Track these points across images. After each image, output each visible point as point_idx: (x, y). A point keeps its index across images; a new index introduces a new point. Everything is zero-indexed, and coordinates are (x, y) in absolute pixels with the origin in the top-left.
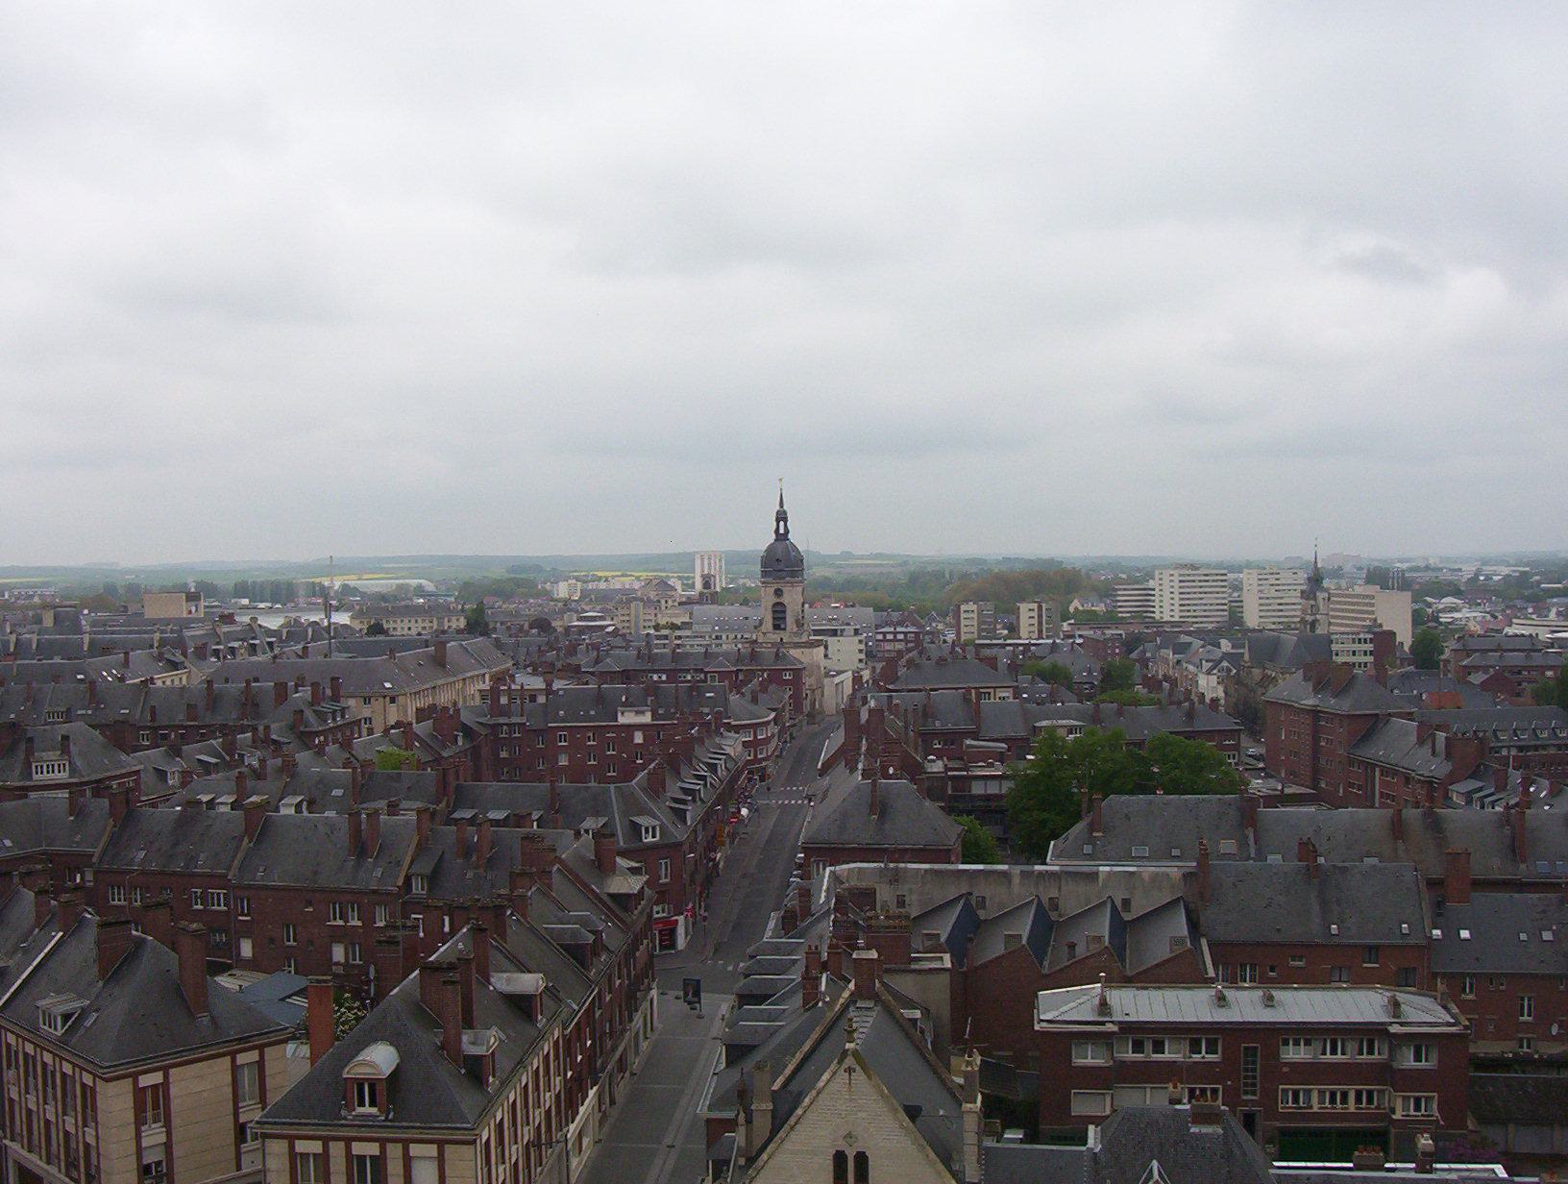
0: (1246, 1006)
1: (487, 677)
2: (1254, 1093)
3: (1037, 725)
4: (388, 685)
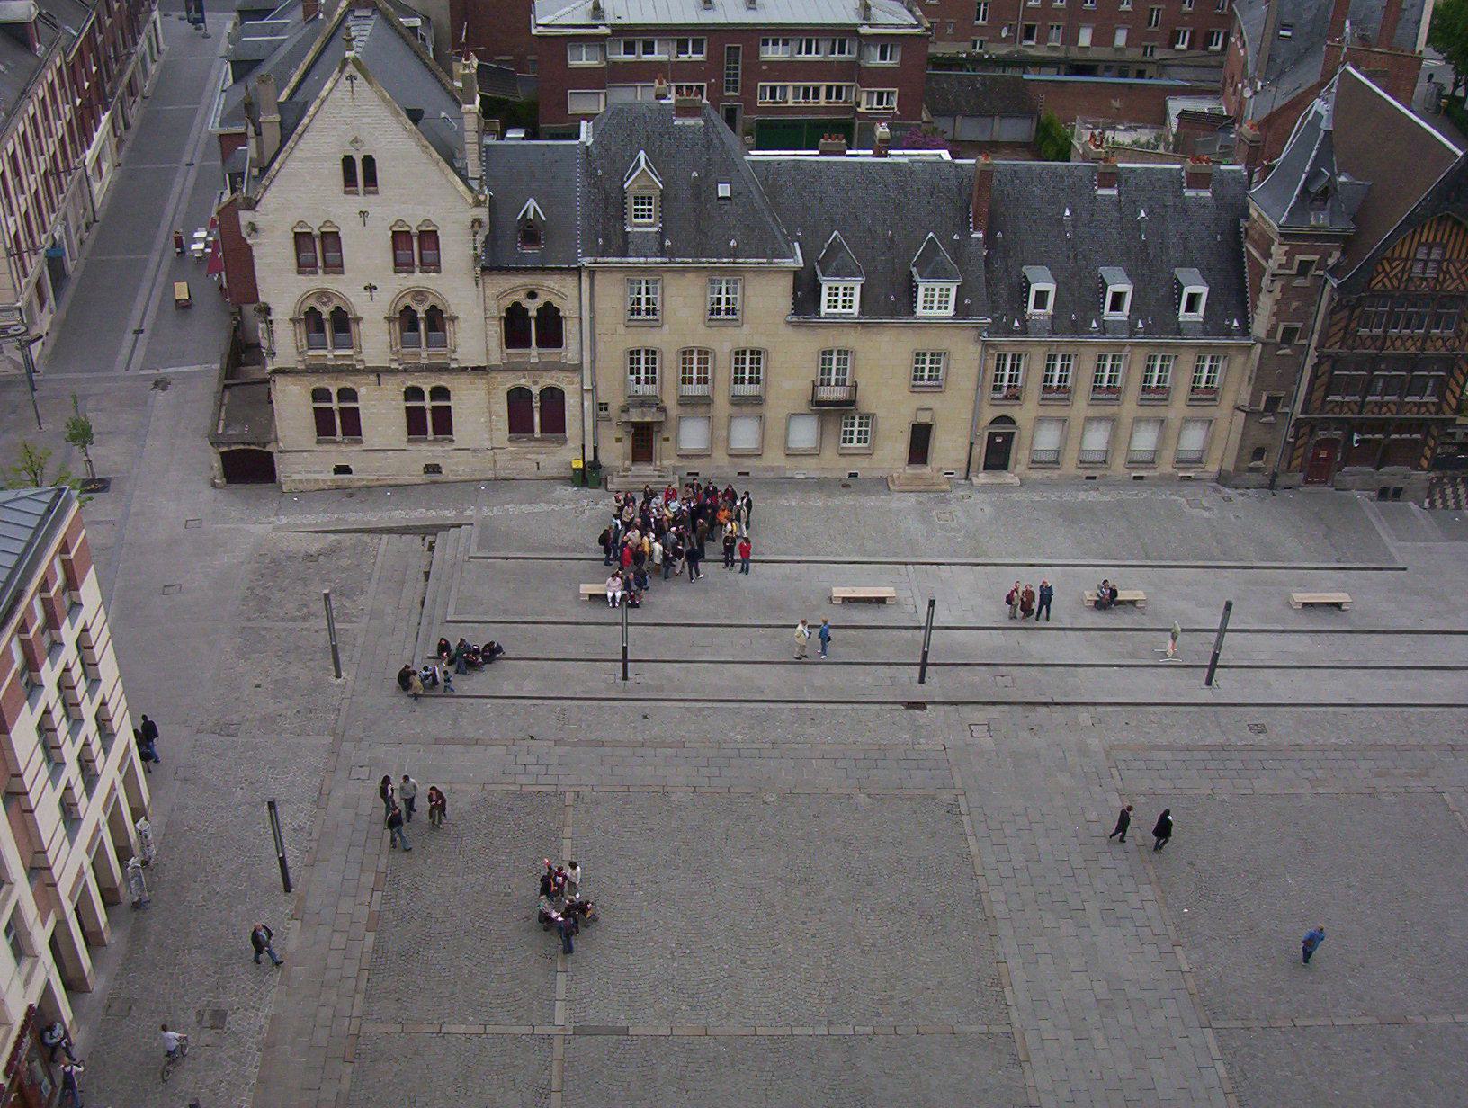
2: (735, 89)
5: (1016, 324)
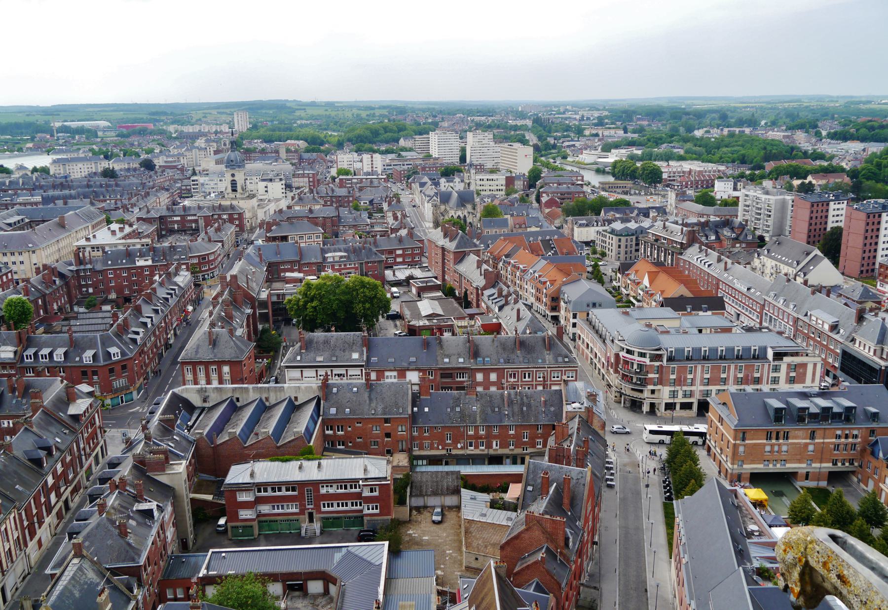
1: (90, 227)
3: (326, 255)
4: (30, 245)
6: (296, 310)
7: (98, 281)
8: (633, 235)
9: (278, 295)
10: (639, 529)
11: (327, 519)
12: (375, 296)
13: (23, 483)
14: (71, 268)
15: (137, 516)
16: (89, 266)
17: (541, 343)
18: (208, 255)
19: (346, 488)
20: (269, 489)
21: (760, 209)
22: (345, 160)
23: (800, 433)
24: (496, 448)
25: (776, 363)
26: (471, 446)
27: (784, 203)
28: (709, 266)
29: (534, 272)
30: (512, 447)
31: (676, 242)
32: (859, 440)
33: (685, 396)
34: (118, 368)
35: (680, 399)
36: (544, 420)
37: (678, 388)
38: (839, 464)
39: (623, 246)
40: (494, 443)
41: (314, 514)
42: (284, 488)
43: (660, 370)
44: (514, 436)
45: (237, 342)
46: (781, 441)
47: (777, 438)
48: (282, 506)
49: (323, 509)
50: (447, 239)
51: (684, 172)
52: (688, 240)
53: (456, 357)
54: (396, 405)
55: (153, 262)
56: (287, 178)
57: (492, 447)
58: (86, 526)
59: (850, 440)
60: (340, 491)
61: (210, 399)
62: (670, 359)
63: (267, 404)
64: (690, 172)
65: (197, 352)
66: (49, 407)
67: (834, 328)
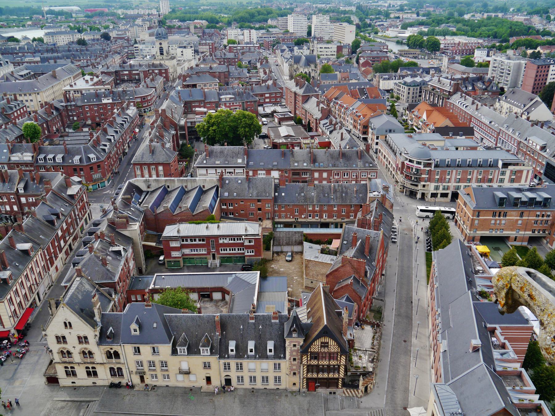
0: (213, 230)
3: (221, 97)
4: (36, 89)
5: (226, 356)
6: (203, 132)
7: (80, 113)
8: (418, 86)
9: (191, 123)
10: (410, 268)
11: (224, 257)
12: (252, 124)
13: (44, 235)
14: (62, 104)
15: (112, 254)
16: (73, 103)
17: (355, 155)
18: (147, 96)
19: (234, 240)
20: (189, 240)
21: (503, 69)
22: (233, 34)
23: (514, 213)
24: (325, 218)
25: (504, 170)
26: (310, 216)
27: (519, 65)
28: (466, 107)
29: (353, 109)
30: (335, 218)
31: (446, 91)
32: (551, 218)
33: (444, 189)
34: (95, 167)
35: (441, 191)
36: (355, 202)
37: (440, 184)
38: (536, 232)
39: (411, 93)
40: (324, 215)
41: (216, 255)
42: (197, 240)
43: (429, 172)
44: (337, 211)
45: (167, 152)
46: (502, 218)
47: (499, 216)
48: (197, 250)
49: (221, 252)
50: (298, 87)
51: (455, 44)
52: (454, 90)
53: (302, 162)
54: (265, 191)
55: (113, 101)
56: (195, 46)
57: (323, 218)
58: (83, 259)
59: (545, 218)
60: (231, 242)
61: (151, 186)
62: (436, 166)
63: (186, 190)
64: (459, 44)
65: (142, 158)
66: (55, 190)
67: (543, 148)
